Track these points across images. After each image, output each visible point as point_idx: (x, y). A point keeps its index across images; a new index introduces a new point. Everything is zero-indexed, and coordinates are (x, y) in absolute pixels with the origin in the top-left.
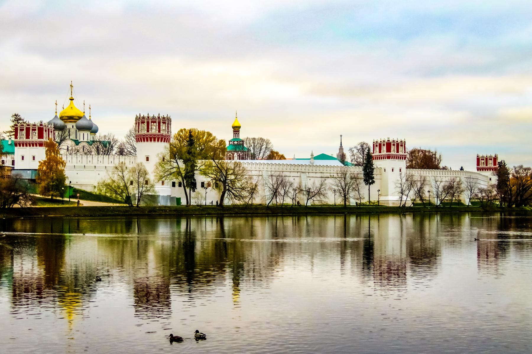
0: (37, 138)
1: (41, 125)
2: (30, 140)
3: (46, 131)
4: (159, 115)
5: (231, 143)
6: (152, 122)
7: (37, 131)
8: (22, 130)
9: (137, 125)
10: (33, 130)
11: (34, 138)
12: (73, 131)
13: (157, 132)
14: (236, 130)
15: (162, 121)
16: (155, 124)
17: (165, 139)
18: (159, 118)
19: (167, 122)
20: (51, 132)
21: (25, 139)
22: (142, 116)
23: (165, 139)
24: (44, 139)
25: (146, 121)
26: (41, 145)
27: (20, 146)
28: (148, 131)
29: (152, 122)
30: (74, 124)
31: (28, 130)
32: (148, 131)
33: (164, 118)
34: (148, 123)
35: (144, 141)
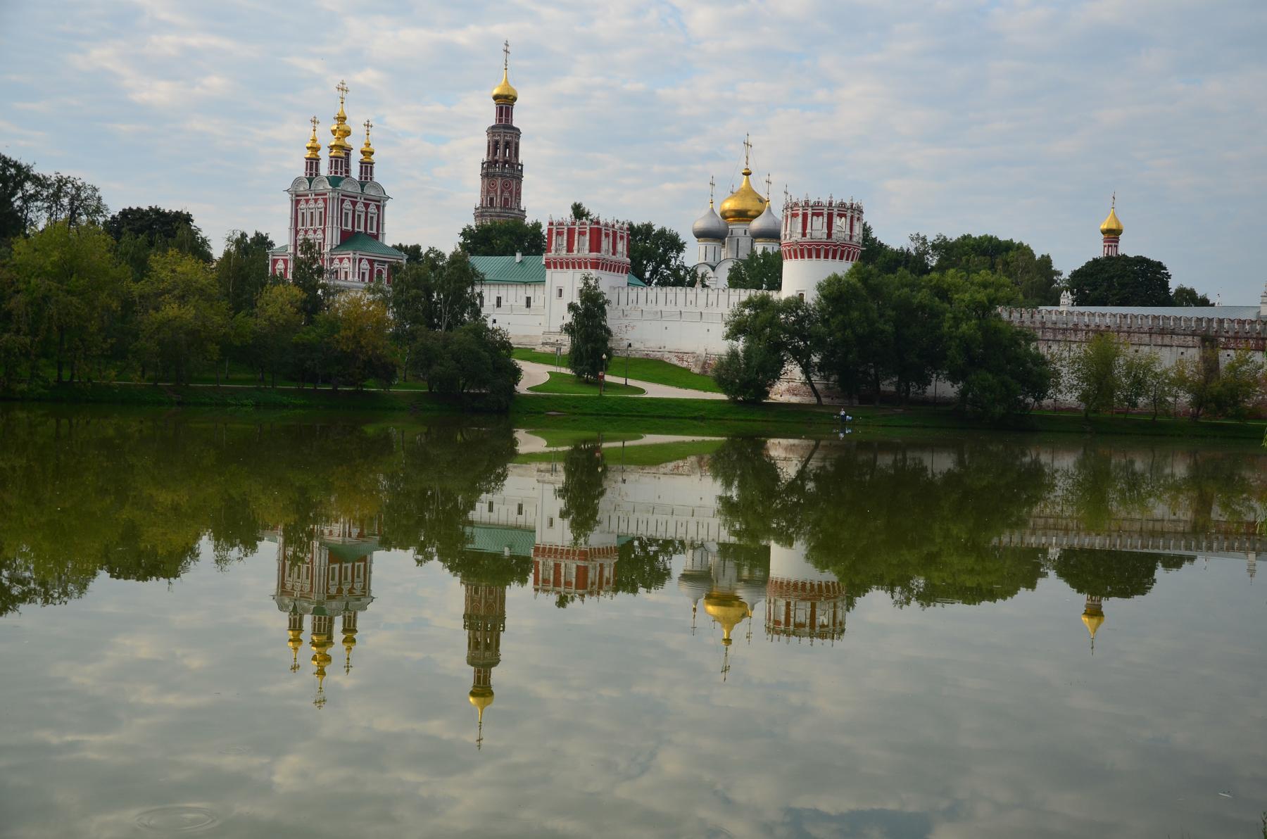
1: (598, 223)
3: (607, 235)
8: (559, 234)
10: (580, 233)
11: (583, 250)
12: (745, 243)
14: (1112, 235)
15: (835, 212)
17: (843, 252)
18: (830, 204)
19: (849, 214)
22: (794, 200)
25: (800, 212)
27: (555, 267)
29: (813, 214)
31: (571, 232)
32: (804, 235)
33: (842, 204)
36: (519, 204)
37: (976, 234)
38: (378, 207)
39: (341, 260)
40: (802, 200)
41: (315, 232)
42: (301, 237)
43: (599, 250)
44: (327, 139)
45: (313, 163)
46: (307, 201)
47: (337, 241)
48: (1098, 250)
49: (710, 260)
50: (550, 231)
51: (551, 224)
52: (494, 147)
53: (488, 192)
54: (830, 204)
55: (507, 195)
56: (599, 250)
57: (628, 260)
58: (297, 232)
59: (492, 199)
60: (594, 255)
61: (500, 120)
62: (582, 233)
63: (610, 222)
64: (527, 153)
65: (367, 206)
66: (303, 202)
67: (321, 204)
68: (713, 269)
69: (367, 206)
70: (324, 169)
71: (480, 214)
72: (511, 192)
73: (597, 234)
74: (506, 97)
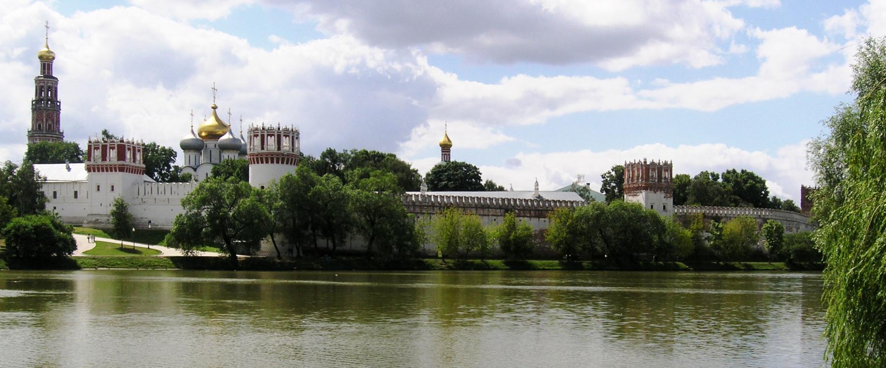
1: (122, 141)
2: (107, 162)
7: (115, 151)
12: (216, 153)
14: (446, 148)
15: (282, 134)
19: (291, 135)
21: (100, 162)
22: (255, 126)
24: (127, 160)
25: (259, 134)
26: (122, 169)
28: (263, 148)
31: (104, 148)
32: (263, 148)
33: (286, 130)
34: (263, 136)
36: (59, 130)
40: (260, 126)
43: (124, 160)
48: (437, 160)
49: (193, 164)
50: (90, 147)
51: (90, 142)
52: (39, 90)
53: (37, 120)
55: (50, 122)
56: (124, 160)
57: (144, 166)
59: (40, 125)
60: (121, 162)
61: (44, 73)
62: (113, 148)
63: (130, 140)
64: (63, 95)
68: (195, 170)
71: (31, 135)
72: (53, 121)
73: (122, 148)
74: (48, 58)
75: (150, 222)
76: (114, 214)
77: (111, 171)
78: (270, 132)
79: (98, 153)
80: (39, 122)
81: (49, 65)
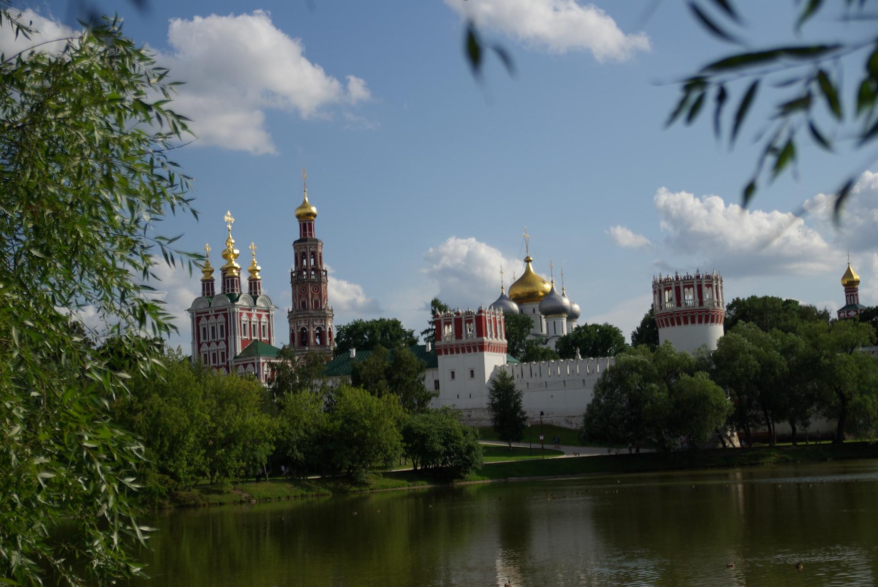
0: (475, 337)
1: (480, 311)
2: (464, 340)
4: (698, 271)
5: (842, 315)
6: (685, 287)
8: (448, 324)
9: (657, 296)
10: (466, 322)
13: (697, 304)
14: (851, 286)
15: (704, 283)
16: (691, 289)
18: (698, 277)
20: (500, 322)
22: (664, 277)
23: (713, 316)
25: (673, 286)
28: (679, 304)
29: (685, 287)
30: (536, 306)
32: (679, 304)
34: (678, 290)
35: (673, 324)
37: (760, 295)
38: (268, 316)
39: (245, 366)
41: (218, 343)
42: (205, 348)
44: (217, 264)
45: (208, 284)
46: (208, 317)
47: (239, 351)
52: (300, 257)
53: (300, 297)
54: (698, 277)
55: (316, 297)
57: (506, 341)
58: (200, 346)
59: (304, 303)
62: (470, 322)
65: (259, 316)
66: (203, 321)
67: (221, 318)
69: (259, 316)
70: (218, 290)
71: (293, 317)
75: (542, 413)
76: (494, 407)
77: (469, 351)
78: (688, 283)
79: (448, 330)
80: (303, 299)
81: (310, 225)
